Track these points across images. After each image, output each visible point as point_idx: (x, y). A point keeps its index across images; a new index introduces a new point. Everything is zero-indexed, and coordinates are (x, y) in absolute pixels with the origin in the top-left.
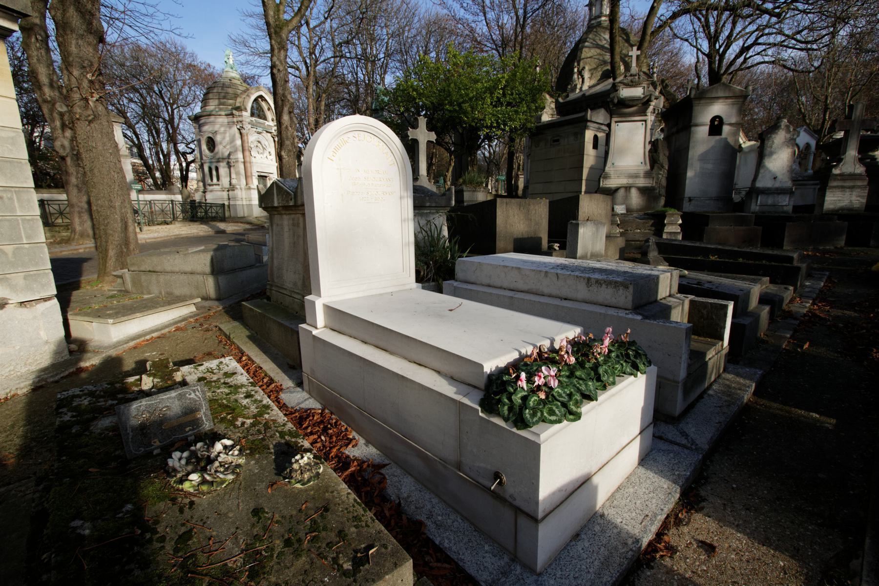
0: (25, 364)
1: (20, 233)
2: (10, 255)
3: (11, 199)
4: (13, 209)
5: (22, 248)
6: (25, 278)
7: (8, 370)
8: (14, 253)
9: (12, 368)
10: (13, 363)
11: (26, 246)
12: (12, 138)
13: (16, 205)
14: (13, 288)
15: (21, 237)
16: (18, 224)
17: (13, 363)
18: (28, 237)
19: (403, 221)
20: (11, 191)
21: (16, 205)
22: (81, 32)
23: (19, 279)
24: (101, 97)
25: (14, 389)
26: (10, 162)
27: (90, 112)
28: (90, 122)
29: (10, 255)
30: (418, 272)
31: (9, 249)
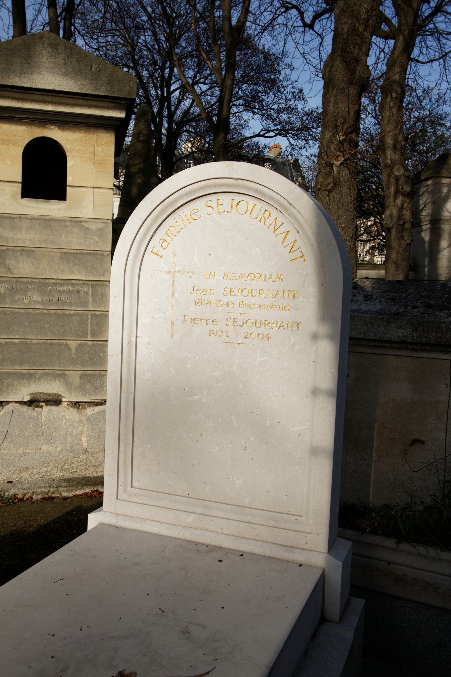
0: (62, 469)
1: (87, 329)
2: (73, 351)
3: (86, 293)
4: (86, 304)
5: (85, 345)
6: (81, 377)
7: (45, 470)
8: (77, 350)
9: (49, 468)
10: (52, 464)
11: (90, 343)
12: (101, 230)
13: (90, 299)
14: (69, 386)
15: (87, 334)
16: (87, 320)
17: (52, 464)
18: (93, 334)
19: (315, 392)
20: (88, 285)
21: (90, 299)
22: (342, 85)
23: (75, 377)
24: (346, 160)
25: (31, 491)
26: (94, 254)
27: (330, 180)
28: (330, 191)
29: (73, 351)
30: (339, 524)
31: (73, 344)
